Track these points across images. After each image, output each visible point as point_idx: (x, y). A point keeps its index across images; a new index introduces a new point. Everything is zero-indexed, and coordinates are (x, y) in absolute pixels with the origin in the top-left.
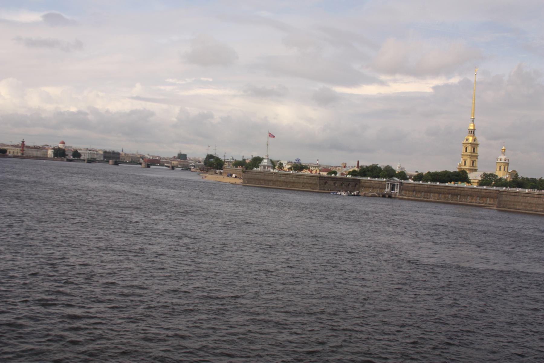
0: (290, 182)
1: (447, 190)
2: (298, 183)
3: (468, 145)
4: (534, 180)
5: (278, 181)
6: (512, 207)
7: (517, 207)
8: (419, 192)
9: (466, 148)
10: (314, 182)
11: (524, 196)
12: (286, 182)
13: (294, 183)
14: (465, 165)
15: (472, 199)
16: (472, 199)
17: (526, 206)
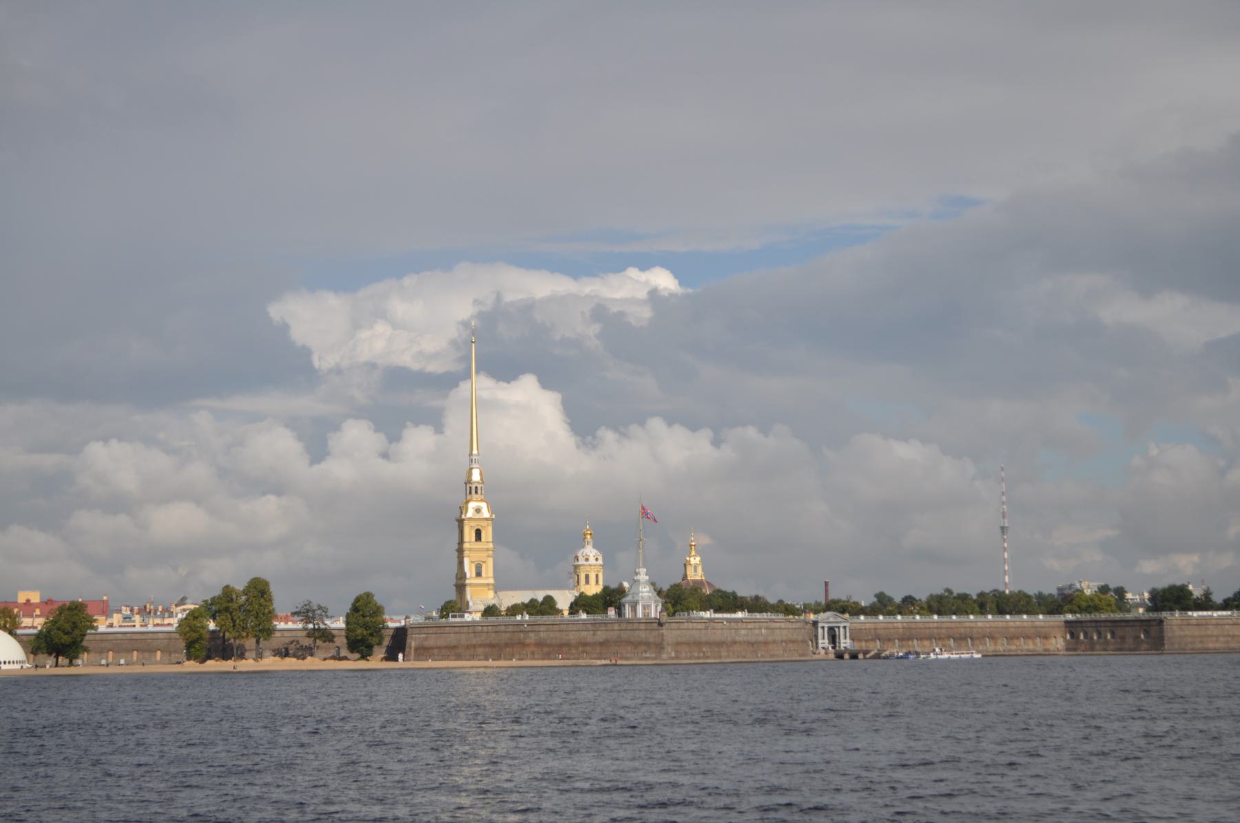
0: (757, 643)
1: (944, 631)
2: (774, 642)
3: (484, 523)
4: (964, 597)
5: (735, 643)
6: (1199, 646)
7: (1211, 646)
8: (889, 640)
9: (478, 533)
10: (800, 638)
11: (1217, 624)
12: (752, 644)
13: (766, 643)
14: (479, 574)
15: (996, 644)
16: (996, 644)
17: (1227, 642)
